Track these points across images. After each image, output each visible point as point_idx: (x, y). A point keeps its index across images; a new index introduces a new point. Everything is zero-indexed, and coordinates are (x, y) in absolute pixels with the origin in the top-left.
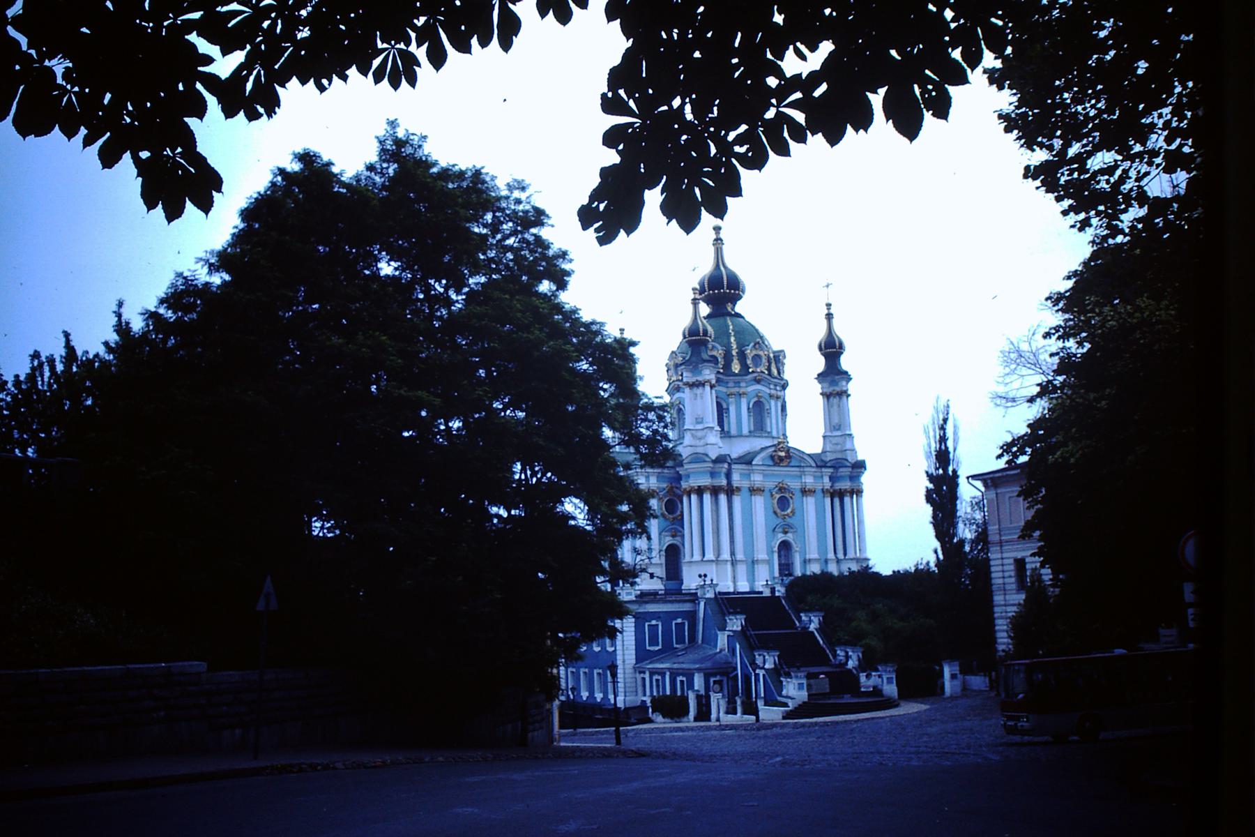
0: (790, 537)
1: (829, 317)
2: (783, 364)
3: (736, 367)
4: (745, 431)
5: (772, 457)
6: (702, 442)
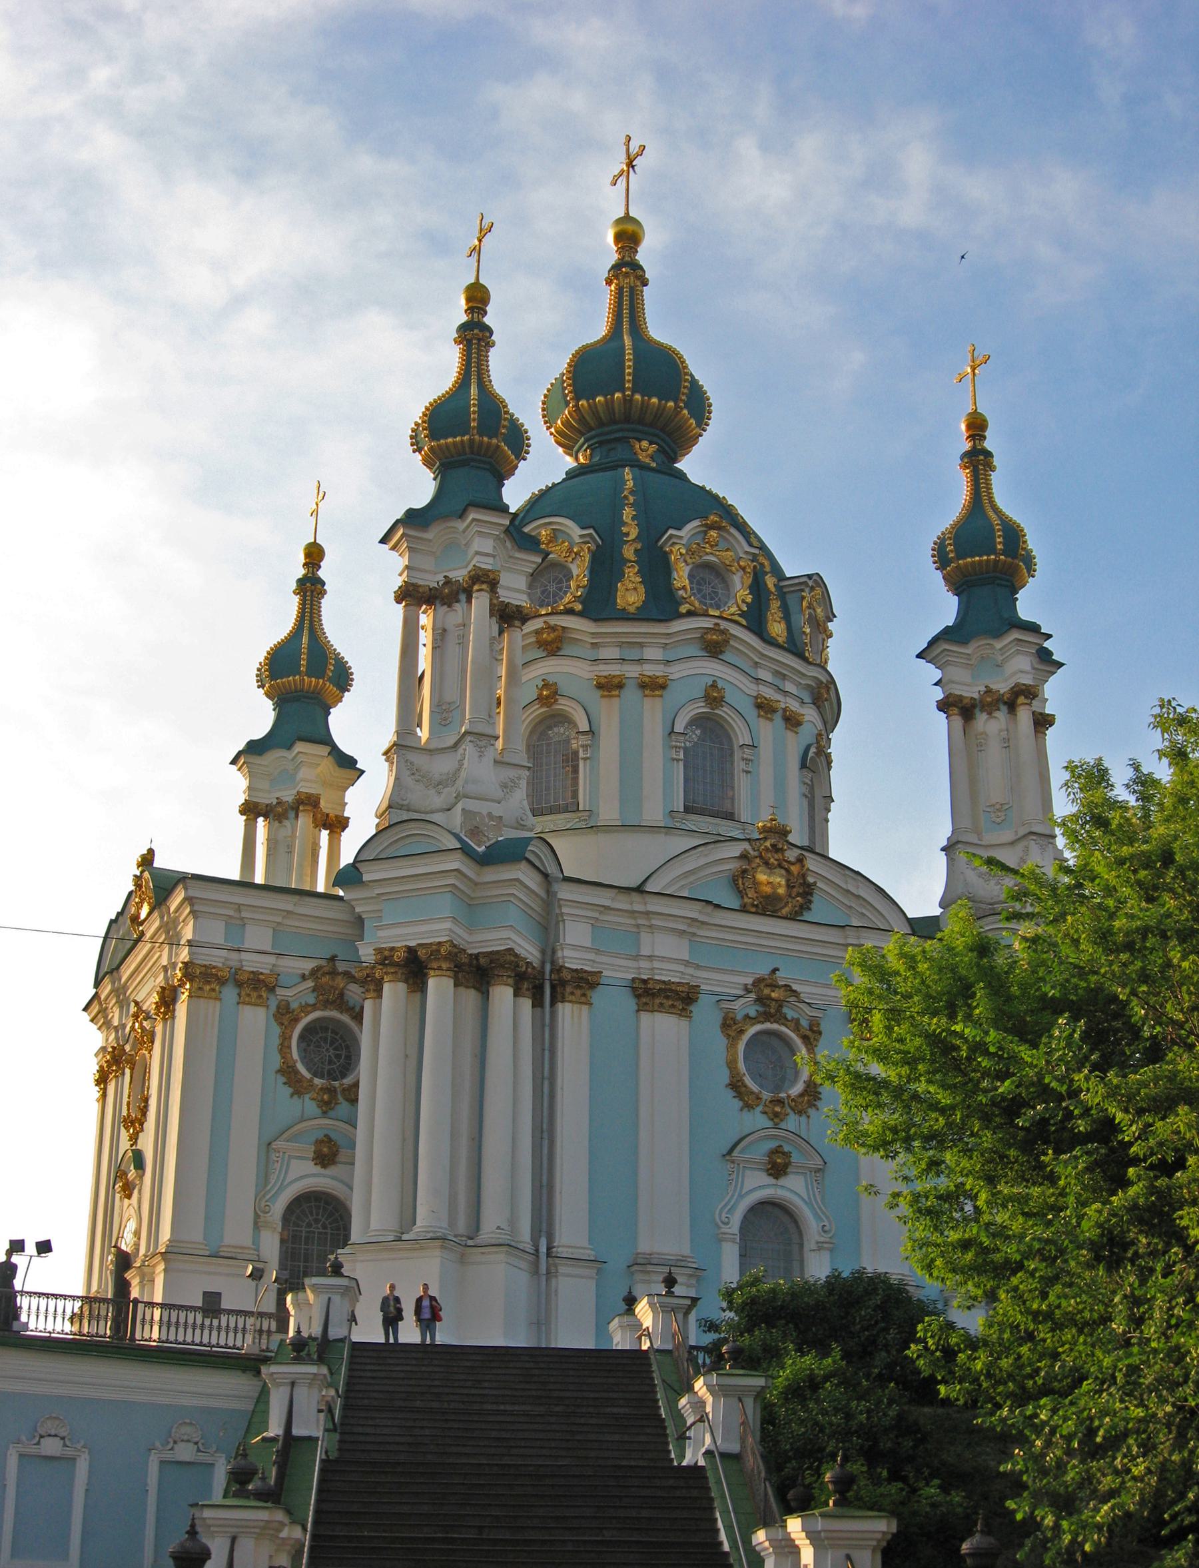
0: (793, 1189)
1: (978, 461)
2: (821, 629)
3: (630, 593)
4: (654, 813)
5: (739, 880)
6: (449, 793)
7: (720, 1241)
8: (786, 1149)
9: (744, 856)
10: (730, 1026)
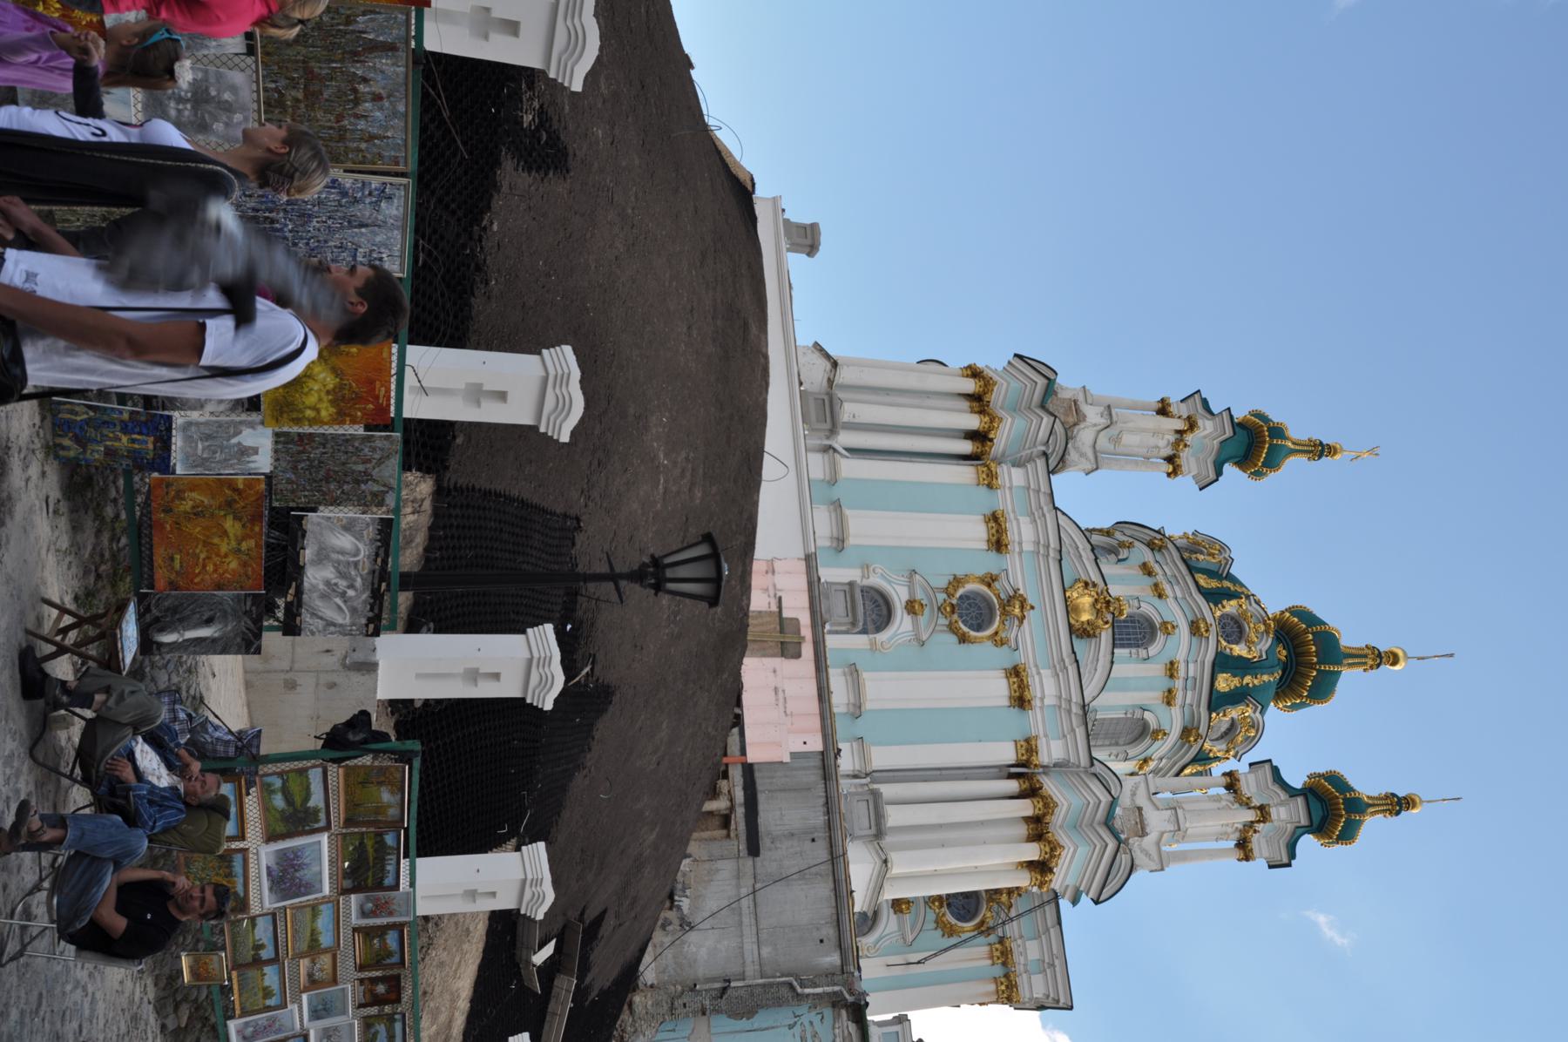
0: (902, 624)
7: (866, 568)
8: (927, 611)
9: (1095, 585)
10: (990, 580)
